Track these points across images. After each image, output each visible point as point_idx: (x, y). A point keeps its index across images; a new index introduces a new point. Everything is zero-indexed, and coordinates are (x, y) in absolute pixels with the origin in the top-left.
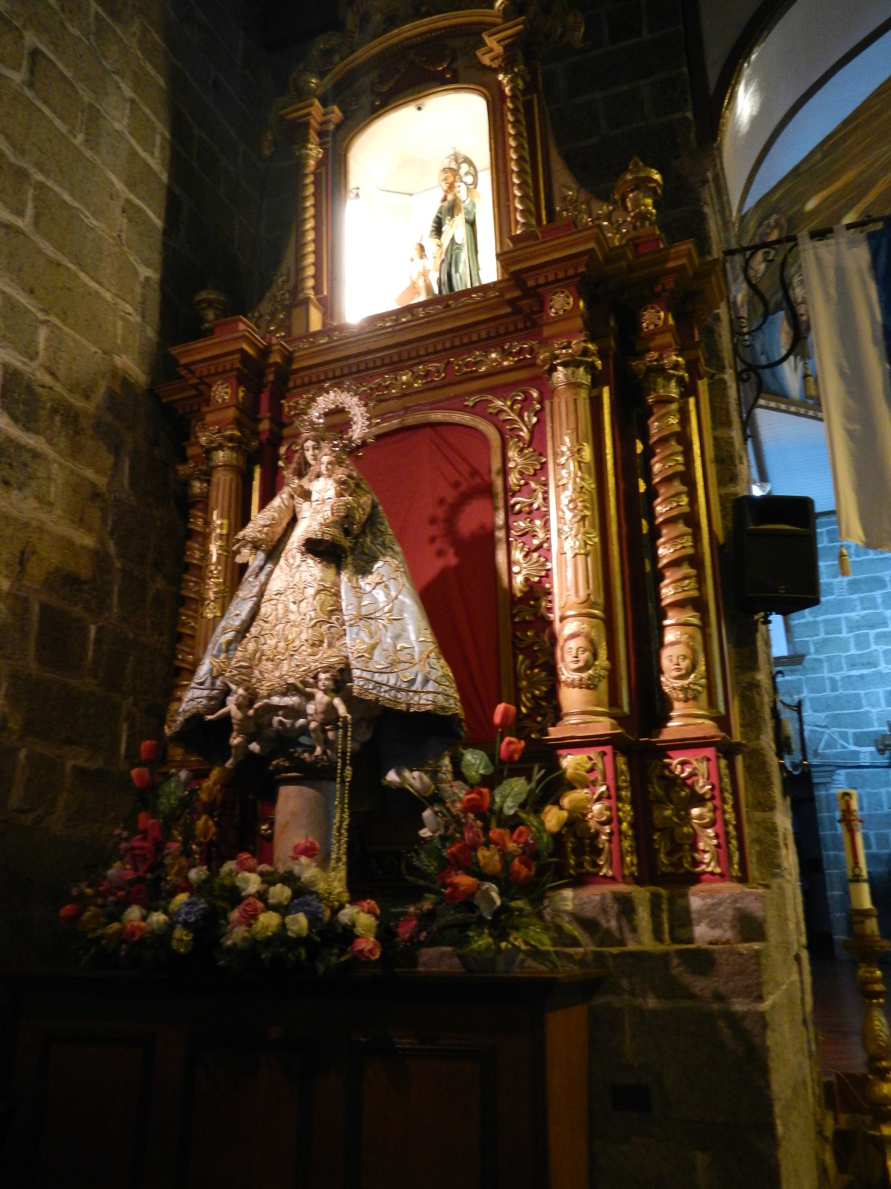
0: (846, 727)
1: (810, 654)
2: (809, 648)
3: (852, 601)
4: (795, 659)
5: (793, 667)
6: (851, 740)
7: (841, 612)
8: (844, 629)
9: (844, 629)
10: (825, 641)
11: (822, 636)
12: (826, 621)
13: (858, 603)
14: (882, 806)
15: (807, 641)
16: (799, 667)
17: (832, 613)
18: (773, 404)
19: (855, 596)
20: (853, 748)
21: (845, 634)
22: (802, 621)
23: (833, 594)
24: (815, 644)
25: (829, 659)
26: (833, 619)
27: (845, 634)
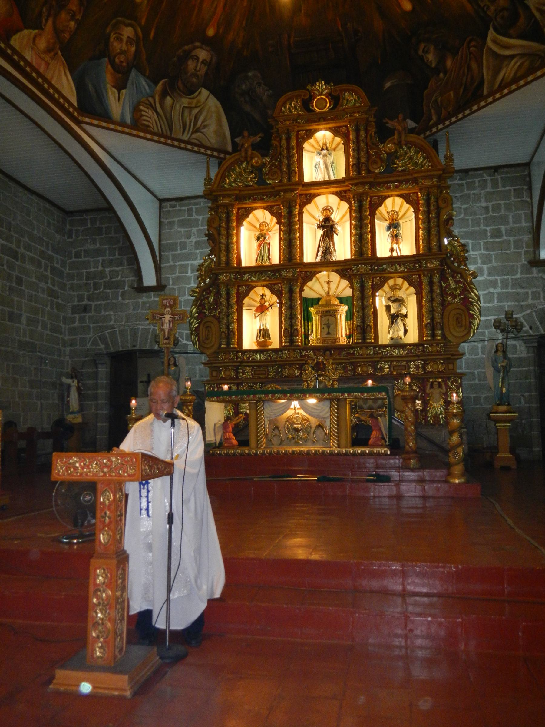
0: (183, 330)
1: (169, 285)
2: (169, 281)
3: (197, 253)
4: (160, 287)
5: (159, 293)
6: (184, 337)
7: (189, 260)
8: (189, 271)
9: (189, 271)
10: (178, 278)
11: (177, 274)
12: (181, 266)
13: (199, 255)
14: (195, 376)
15: (169, 278)
16: (163, 293)
17: (184, 261)
18: (96, 122)
19: (198, 251)
20: (185, 342)
21: (189, 274)
22: (167, 265)
23: (186, 249)
24: (173, 279)
25: (179, 289)
26: (183, 265)
27: (189, 274)
